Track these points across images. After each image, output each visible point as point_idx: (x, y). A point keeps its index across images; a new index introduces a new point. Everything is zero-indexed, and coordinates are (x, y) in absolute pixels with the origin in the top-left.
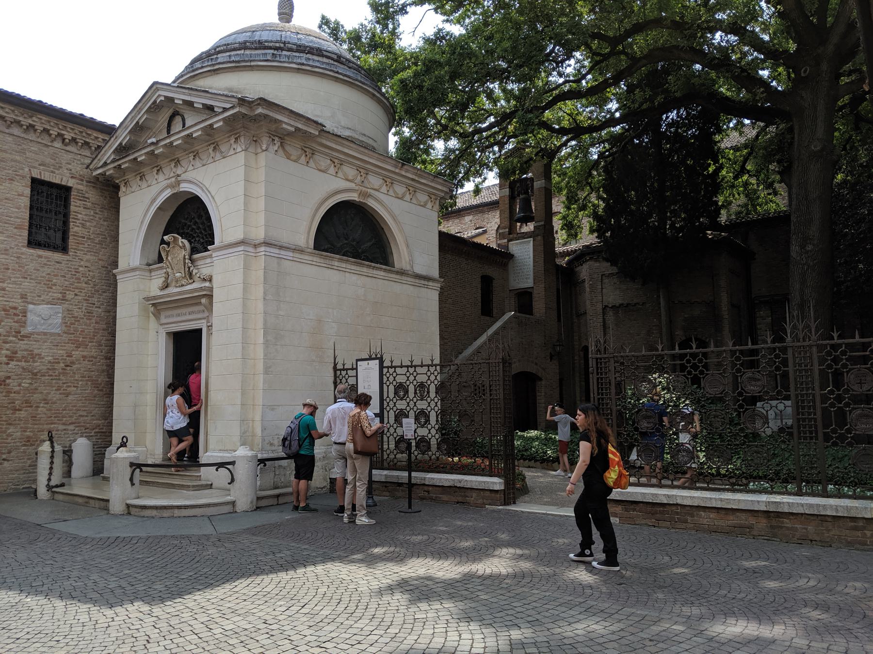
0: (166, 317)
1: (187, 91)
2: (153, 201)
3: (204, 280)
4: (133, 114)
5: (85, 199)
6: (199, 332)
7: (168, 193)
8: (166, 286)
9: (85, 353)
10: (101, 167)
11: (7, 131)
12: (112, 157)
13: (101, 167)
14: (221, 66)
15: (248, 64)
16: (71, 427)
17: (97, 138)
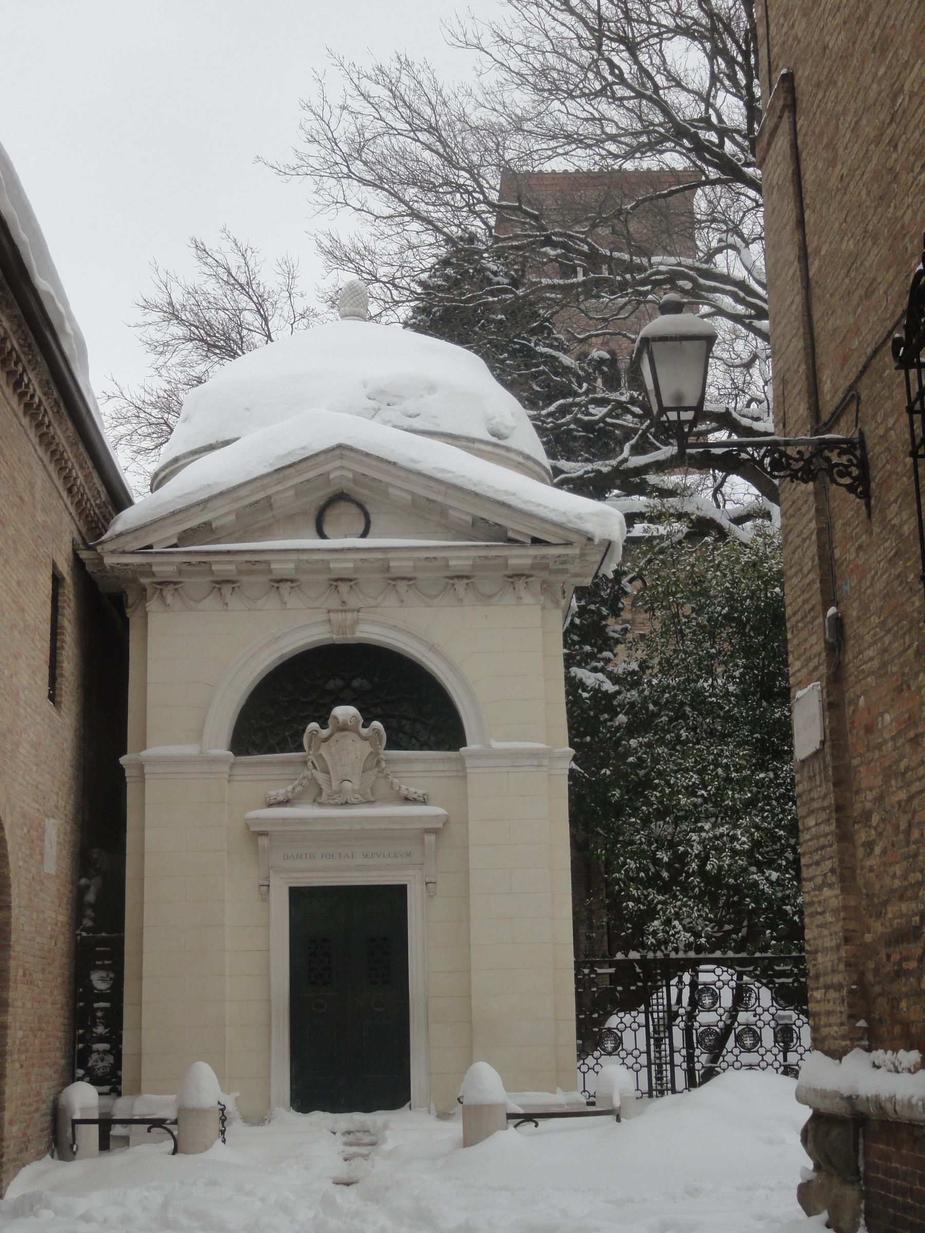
4: (265, 482)
6: (399, 893)
10: (133, 553)
12: (175, 541)
13: (133, 553)
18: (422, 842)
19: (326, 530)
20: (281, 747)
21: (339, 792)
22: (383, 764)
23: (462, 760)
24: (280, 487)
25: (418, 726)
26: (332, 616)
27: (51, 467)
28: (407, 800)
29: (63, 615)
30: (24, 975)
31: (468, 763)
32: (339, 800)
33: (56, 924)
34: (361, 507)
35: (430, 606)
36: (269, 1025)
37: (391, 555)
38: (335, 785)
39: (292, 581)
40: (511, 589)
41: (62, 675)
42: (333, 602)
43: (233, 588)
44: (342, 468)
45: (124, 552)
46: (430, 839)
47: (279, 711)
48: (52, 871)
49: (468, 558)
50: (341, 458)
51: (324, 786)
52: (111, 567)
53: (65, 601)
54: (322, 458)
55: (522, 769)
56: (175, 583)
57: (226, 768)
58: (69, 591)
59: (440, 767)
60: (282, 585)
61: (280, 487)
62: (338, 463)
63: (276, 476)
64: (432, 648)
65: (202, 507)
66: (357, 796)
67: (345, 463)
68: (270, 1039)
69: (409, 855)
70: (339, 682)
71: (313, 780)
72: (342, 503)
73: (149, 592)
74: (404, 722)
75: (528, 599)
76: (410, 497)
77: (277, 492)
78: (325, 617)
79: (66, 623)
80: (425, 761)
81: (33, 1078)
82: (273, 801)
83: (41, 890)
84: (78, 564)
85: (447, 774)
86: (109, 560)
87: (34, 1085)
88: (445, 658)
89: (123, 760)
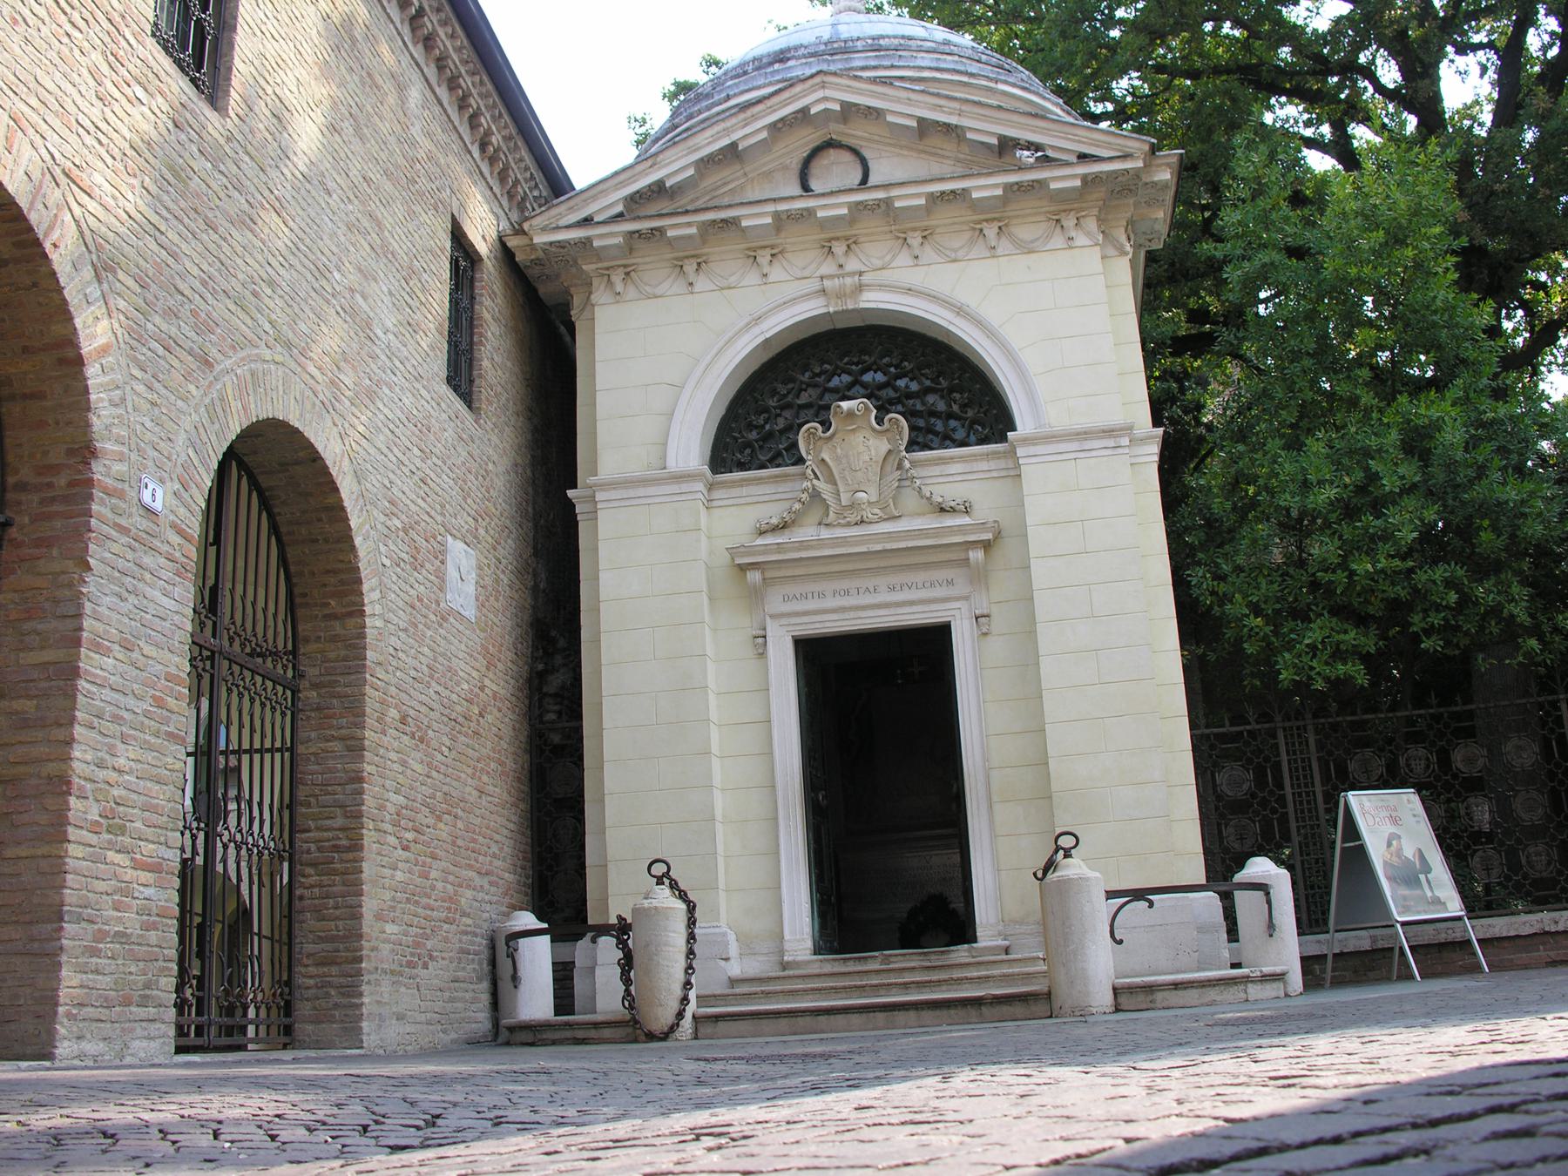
0: (787, 599)
1: (956, 105)
2: (758, 320)
3: (953, 510)
4: (728, 124)
5: (493, 296)
7: (812, 308)
8: (783, 526)
9: (495, 687)
10: (568, 227)
11: (438, 90)
12: (620, 208)
13: (568, 227)
14: (938, 75)
15: (992, 85)
16: (485, 882)
17: (521, 160)
18: (966, 561)
19: (815, 185)
20: (774, 460)
21: (852, 506)
22: (907, 464)
23: (1012, 452)
24: (748, 130)
25: (953, 423)
26: (827, 283)
27: (442, 92)
28: (942, 510)
29: (481, 304)
30: (403, 721)
31: (1020, 452)
32: (853, 518)
33: (482, 689)
34: (855, 152)
35: (955, 261)
36: (776, 819)
37: (895, 192)
38: (845, 499)
39: (772, 247)
40: (1058, 229)
41: (480, 376)
42: (828, 268)
43: (699, 264)
44: (825, 99)
45: (558, 228)
46: (977, 555)
47: (765, 417)
48: (470, 613)
49: (996, 186)
50: (823, 86)
51: (830, 500)
52: (544, 251)
53: (483, 288)
54: (798, 88)
55: (1094, 453)
56: (625, 266)
57: (700, 486)
58: (490, 274)
59: (984, 466)
60: (760, 252)
61: (748, 130)
62: (820, 94)
63: (742, 116)
64: (960, 311)
65: (650, 162)
66: (876, 511)
67: (828, 93)
68: (777, 837)
69: (950, 583)
70: (846, 378)
71: (815, 495)
72: (832, 151)
73: (595, 282)
74: (933, 420)
75: (1082, 240)
76: (915, 124)
77: (745, 137)
78: (816, 285)
79: (486, 315)
80: (962, 459)
81: (434, 874)
82: (764, 527)
83: (441, 626)
84: (506, 253)
85: (995, 474)
86: (537, 240)
87: (440, 885)
88: (979, 323)
89: (570, 493)
